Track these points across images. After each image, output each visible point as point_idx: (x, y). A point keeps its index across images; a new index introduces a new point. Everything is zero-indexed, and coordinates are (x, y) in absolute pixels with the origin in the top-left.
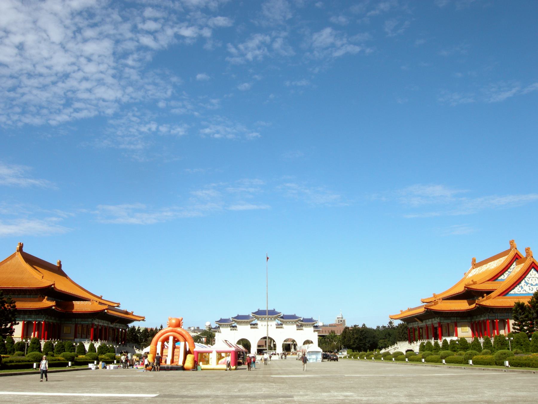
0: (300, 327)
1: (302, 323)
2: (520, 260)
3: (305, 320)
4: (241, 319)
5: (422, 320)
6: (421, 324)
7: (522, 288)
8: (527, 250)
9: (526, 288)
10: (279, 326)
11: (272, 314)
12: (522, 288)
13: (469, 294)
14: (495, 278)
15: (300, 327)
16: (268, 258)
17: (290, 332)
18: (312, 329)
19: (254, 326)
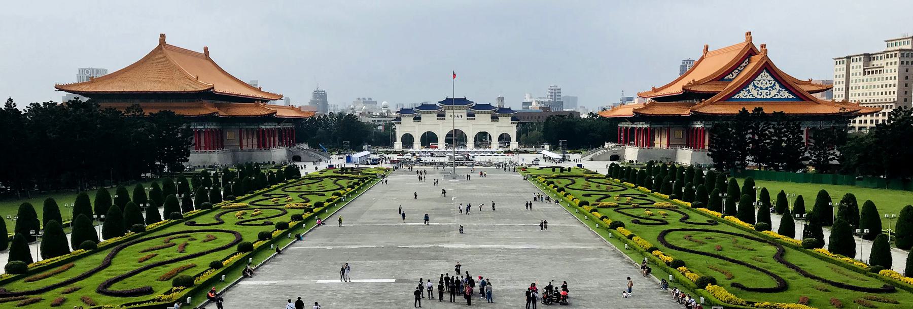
0: (495, 118)
1: (498, 112)
4: (427, 108)
6: (630, 125)
7: (749, 92)
8: (763, 46)
9: (754, 93)
10: (471, 116)
11: (462, 102)
13: (688, 95)
14: (721, 78)
15: (495, 118)
16: (454, 75)
17: (483, 123)
19: (441, 116)
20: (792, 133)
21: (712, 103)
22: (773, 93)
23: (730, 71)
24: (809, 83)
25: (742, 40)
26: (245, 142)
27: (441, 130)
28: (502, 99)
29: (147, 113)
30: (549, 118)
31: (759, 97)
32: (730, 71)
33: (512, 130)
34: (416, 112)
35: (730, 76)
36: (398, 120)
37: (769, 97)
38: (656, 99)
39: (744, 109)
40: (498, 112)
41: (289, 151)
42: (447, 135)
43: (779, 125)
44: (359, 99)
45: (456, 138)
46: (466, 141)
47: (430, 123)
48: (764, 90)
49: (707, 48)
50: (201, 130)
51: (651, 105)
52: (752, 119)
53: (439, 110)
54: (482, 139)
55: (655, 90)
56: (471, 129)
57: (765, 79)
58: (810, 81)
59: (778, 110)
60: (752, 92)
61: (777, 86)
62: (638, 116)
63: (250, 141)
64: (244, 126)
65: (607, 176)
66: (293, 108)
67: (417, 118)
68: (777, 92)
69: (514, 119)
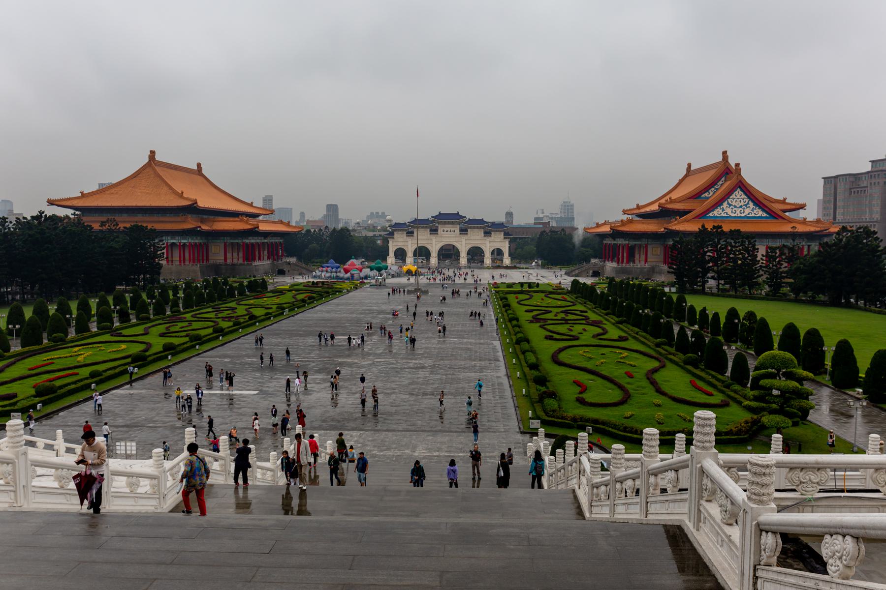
0: (487, 233)
2: (730, 175)
3: (494, 225)
4: (418, 223)
5: (614, 239)
7: (723, 210)
8: (737, 165)
9: (729, 211)
10: (464, 231)
12: (723, 210)
13: (664, 213)
14: (696, 196)
15: (487, 233)
17: (476, 238)
18: (502, 235)
19: (434, 231)
20: (746, 250)
21: (687, 221)
22: (747, 211)
23: (707, 189)
24: (783, 201)
25: (720, 159)
26: (229, 255)
27: (434, 245)
28: (509, 215)
29: (121, 226)
30: (543, 233)
31: (733, 215)
32: (707, 189)
33: (505, 247)
34: (410, 228)
35: (706, 195)
36: (391, 234)
37: (743, 215)
38: (639, 216)
39: (703, 226)
40: (489, 228)
41: (272, 264)
42: (441, 249)
43: (735, 243)
44: (372, 213)
45: (449, 254)
46: (459, 256)
47: (424, 238)
48: (736, 210)
49: (689, 165)
50: (184, 244)
51: (630, 221)
52: (712, 236)
53: (432, 225)
54: (476, 254)
55: (638, 207)
56: (463, 245)
57: (738, 197)
58: (785, 199)
59: (734, 227)
60: (725, 211)
61: (751, 205)
62: (616, 234)
63: (235, 255)
64: (229, 240)
65: (568, 292)
66: (281, 222)
67: (410, 234)
68: (752, 211)
69: (507, 234)
